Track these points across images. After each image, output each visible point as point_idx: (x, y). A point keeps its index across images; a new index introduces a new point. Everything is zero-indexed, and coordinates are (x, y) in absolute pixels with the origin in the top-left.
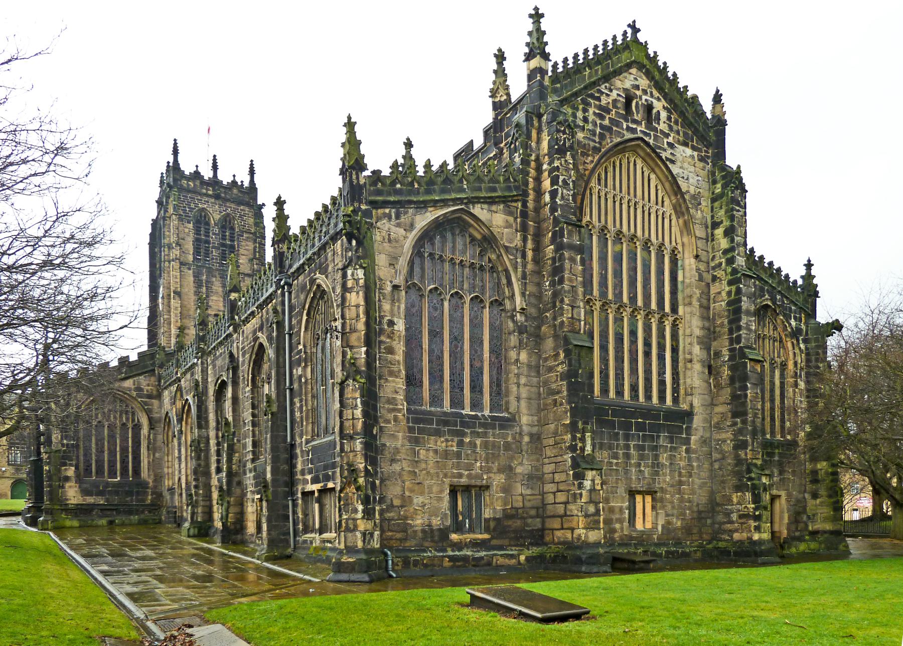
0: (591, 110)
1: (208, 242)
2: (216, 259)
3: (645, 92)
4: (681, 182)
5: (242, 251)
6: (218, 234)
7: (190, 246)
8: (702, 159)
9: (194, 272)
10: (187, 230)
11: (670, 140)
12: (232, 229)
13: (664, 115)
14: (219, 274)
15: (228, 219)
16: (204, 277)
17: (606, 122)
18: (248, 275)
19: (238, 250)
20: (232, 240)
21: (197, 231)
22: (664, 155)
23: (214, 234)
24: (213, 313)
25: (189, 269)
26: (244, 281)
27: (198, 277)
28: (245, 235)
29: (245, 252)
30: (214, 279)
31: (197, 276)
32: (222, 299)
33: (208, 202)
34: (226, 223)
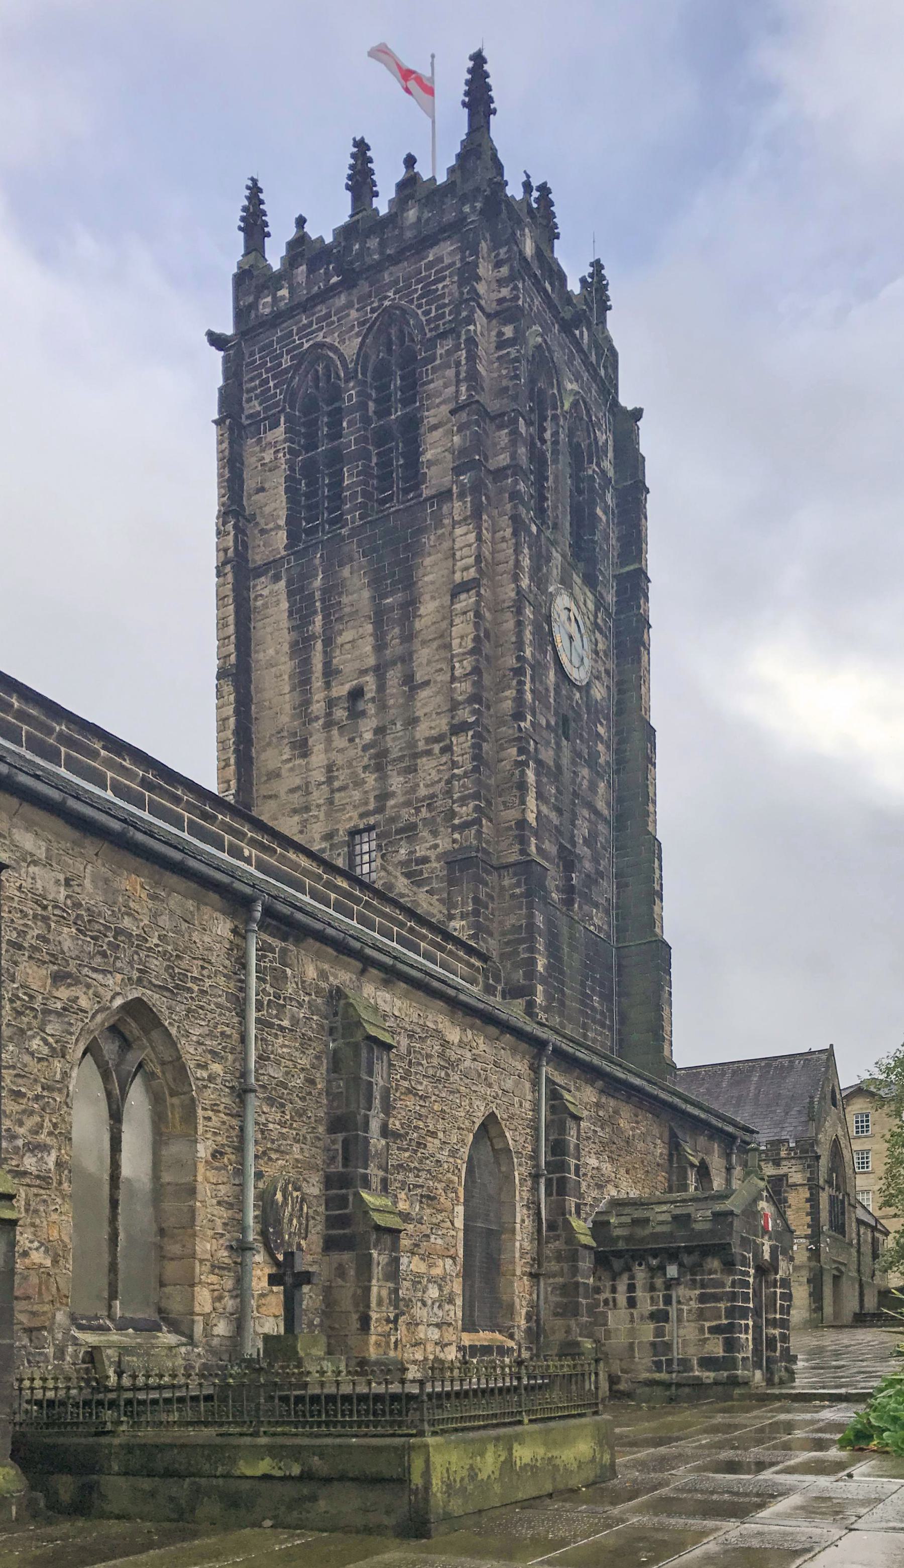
9: (289, 583)
24: (347, 687)
27: (302, 589)
32: (369, 628)
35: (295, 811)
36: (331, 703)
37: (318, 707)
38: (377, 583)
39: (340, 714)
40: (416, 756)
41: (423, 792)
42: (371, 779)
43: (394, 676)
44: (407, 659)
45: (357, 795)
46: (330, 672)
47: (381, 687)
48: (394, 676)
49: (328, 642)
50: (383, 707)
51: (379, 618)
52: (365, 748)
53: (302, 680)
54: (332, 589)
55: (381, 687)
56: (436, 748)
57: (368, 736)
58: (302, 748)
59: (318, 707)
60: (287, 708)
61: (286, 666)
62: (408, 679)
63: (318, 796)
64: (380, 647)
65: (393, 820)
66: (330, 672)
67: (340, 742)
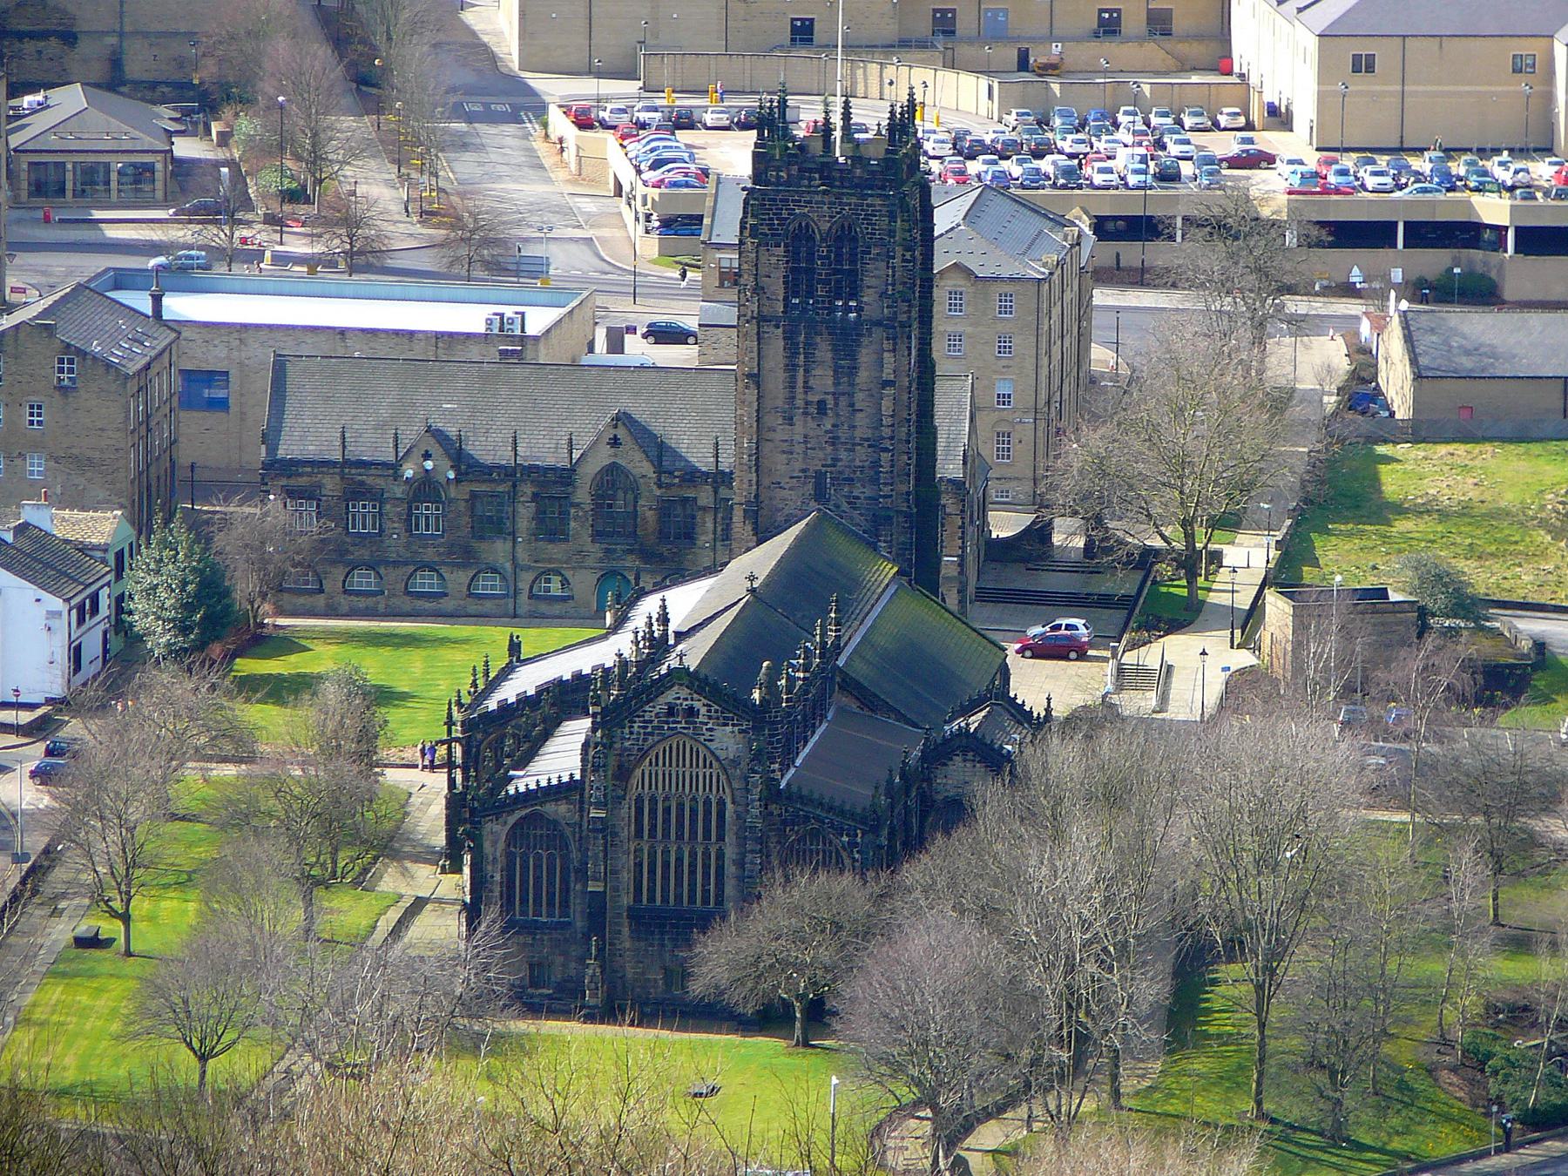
0: (636, 725)
1: (810, 271)
2: (823, 302)
3: (686, 699)
4: (718, 753)
5: (868, 281)
6: (828, 257)
7: (777, 287)
8: (741, 732)
9: (784, 332)
10: (774, 260)
11: (709, 726)
12: (855, 239)
13: (703, 710)
14: (827, 328)
15: (846, 224)
16: (802, 338)
17: (649, 730)
18: (879, 323)
19: (862, 280)
20: (853, 262)
21: (793, 255)
22: (702, 738)
23: (821, 258)
24: (816, 399)
25: (777, 327)
26: (870, 336)
28: (874, 251)
29: (873, 282)
30: (818, 339)
31: (789, 337)
33: (810, 202)
34: (844, 236)
35: (784, 452)
36: (807, 403)
37: (799, 402)
38: (835, 350)
39: (813, 410)
40: (854, 444)
41: (858, 463)
42: (829, 449)
43: (843, 401)
44: (851, 395)
45: (821, 454)
46: (807, 388)
47: (836, 404)
48: (843, 401)
49: (806, 371)
50: (838, 415)
51: (837, 370)
52: (826, 432)
53: (792, 386)
54: (809, 344)
55: (836, 404)
56: (866, 444)
57: (829, 427)
58: (790, 420)
59: (799, 402)
60: (781, 396)
61: (781, 375)
62: (852, 405)
63: (799, 449)
64: (836, 384)
65: (840, 473)
66: (807, 388)
67: (812, 424)
